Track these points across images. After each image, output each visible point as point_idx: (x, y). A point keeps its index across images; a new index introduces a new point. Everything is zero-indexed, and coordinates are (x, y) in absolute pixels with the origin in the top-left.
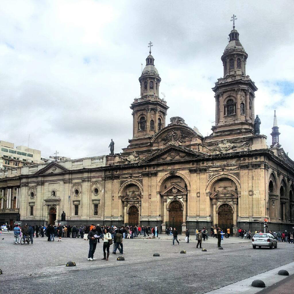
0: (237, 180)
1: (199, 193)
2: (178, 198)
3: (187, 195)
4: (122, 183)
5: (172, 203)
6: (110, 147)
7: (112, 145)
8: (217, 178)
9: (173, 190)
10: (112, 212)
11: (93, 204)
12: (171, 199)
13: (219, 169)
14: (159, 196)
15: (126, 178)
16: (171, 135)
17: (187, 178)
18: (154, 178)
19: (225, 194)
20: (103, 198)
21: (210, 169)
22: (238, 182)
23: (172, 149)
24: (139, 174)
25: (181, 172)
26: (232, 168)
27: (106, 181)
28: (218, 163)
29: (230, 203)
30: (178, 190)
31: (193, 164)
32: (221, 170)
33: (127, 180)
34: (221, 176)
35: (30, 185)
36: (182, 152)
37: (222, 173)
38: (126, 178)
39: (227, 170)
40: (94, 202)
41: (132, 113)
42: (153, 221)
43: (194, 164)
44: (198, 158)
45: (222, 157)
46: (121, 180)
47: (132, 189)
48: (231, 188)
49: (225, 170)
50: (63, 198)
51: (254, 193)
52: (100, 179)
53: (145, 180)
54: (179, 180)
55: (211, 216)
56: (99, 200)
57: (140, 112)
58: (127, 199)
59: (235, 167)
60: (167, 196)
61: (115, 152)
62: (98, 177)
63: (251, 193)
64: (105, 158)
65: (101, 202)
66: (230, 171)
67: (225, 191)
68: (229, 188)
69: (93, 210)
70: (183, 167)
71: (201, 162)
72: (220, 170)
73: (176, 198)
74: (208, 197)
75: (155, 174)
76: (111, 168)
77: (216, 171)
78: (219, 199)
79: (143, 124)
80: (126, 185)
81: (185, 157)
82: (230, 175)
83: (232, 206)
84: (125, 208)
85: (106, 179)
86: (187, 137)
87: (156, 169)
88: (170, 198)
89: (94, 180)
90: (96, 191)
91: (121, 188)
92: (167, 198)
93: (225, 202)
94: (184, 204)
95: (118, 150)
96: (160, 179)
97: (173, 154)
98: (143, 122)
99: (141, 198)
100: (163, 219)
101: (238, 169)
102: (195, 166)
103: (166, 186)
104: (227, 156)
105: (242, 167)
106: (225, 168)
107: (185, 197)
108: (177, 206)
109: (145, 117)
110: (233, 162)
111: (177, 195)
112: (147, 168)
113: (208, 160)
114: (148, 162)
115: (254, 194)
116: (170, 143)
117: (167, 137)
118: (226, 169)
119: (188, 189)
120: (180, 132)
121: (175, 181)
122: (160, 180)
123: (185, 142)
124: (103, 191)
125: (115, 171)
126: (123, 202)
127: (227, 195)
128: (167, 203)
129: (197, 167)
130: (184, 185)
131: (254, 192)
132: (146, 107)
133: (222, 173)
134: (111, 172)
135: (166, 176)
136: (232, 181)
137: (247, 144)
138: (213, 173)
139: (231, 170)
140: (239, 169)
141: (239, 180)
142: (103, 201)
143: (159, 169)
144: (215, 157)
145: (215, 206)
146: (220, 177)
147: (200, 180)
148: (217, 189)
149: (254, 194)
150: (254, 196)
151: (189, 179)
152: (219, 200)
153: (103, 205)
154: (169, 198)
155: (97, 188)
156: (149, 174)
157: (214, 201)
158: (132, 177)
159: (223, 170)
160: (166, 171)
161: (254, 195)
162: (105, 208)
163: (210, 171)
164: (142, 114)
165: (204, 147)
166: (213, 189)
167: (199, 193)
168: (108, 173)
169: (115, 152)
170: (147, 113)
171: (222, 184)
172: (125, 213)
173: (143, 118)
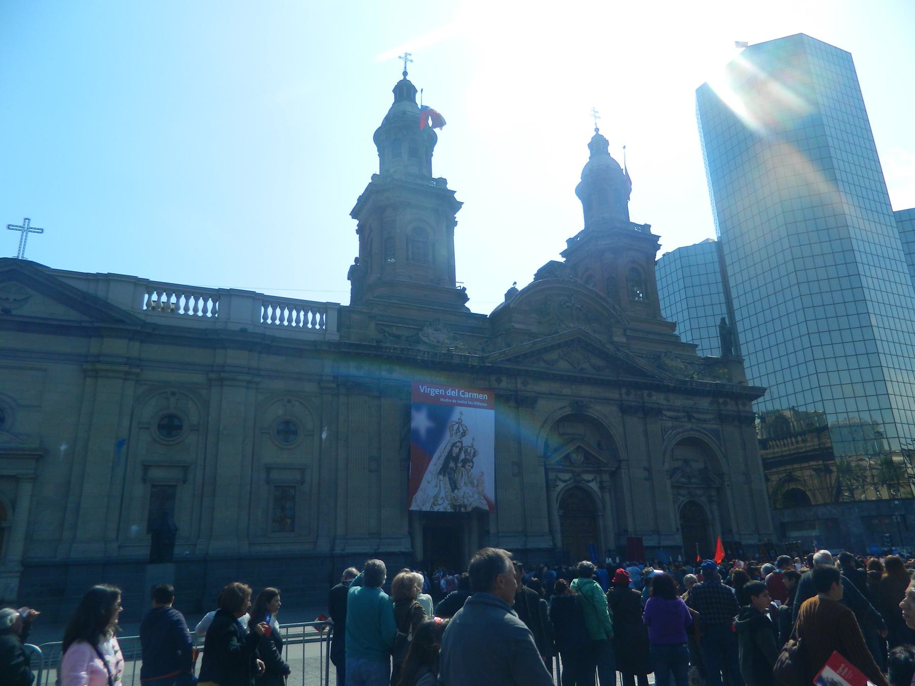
2: (584, 480)
11: (268, 482)
12: (565, 481)
28: (680, 401)
31: (628, 394)
32: (686, 419)
37: (689, 426)
49: (693, 420)
50: (63, 447)
56: (302, 470)
64: (334, 315)
71: (646, 392)
77: (676, 419)
88: (563, 478)
105: (722, 418)
107: (606, 477)
110: (705, 403)
112: (504, 379)
124: (324, 436)
133: (689, 426)
139: (705, 421)
163: (664, 418)
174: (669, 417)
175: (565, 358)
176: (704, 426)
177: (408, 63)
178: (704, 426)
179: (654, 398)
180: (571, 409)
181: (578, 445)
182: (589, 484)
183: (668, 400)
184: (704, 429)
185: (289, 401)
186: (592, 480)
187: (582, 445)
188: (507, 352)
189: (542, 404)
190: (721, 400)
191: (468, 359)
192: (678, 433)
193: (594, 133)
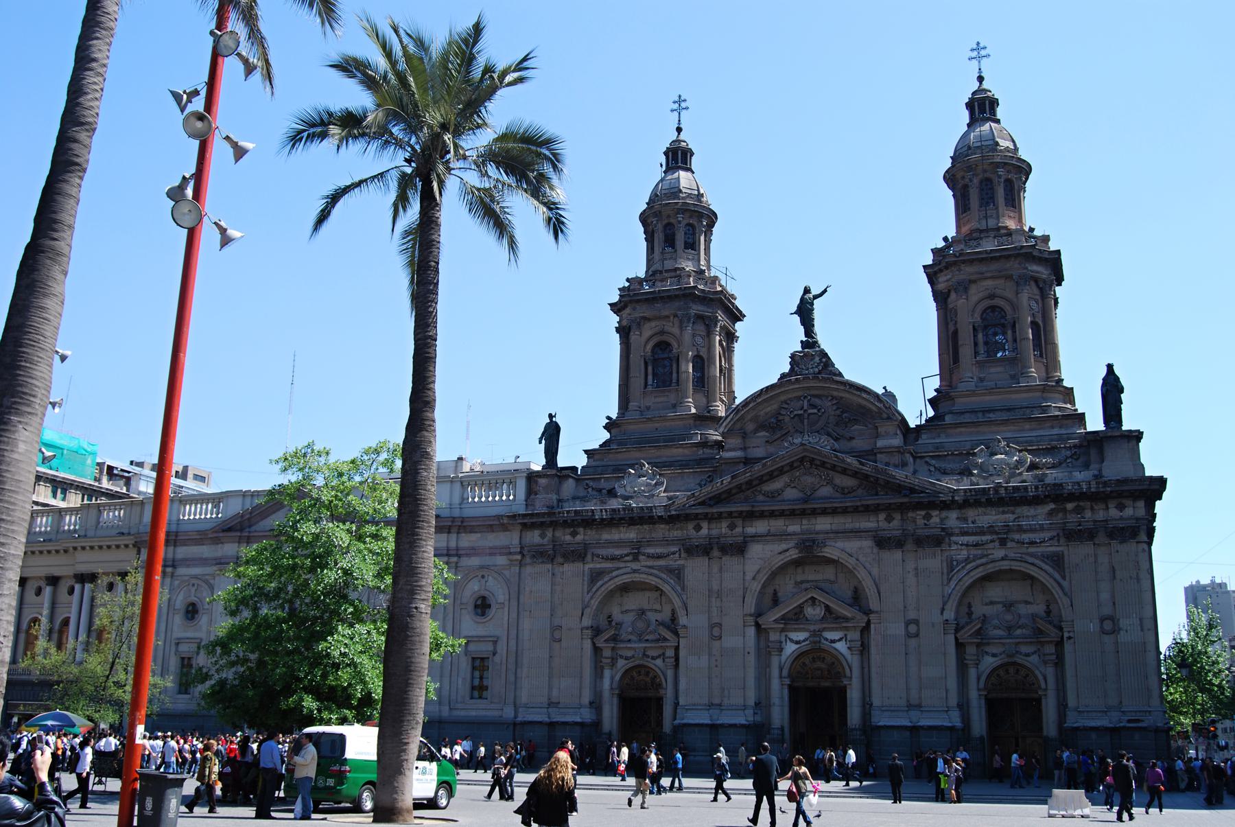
0: (1055, 580)
1: (916, 622)
2: (826, 639)
3: (866, 629)
4: (595, 576)
5: (799, 656)
6: (543, 441)
7: (551, 434)
8: (981, 569)
9: (809, 611)
10: (550, 688)
12: (797, 642)
13: (989, 537)
14: (751, 632)
15: (613, 558)
16: (801, 412)
17: (867, 565)
18: (731, 563)
19: (1009, 628)
20: (513, 632)
21: (954, 538)
22: (1059, 584)
23: (808, 461)
24: (668, 545)
25: (840, 544)
26: (1036, 537)
27: (528, 570)
29: (1031, 659)
30: (827, 608)
31: (889, 519)
32: (997, 544)
33: (618, 569)
34: (997, 564)
35: (181, 571)
36: (844, 471)
37: (1000, 553)
38: (613, 558)
39: (1018, 542)
40: (472, 647)
41: (617, 325)
42: (731, 726)
43: (894, 519)
44: (915, 498)
45: (1001, 499)
46: (591, 566)
47: (635, 601)
48: (1028, 606)
49: (1009, 544)
51: (1121, 626)
52: (501, 560)
53: (696, 570)
54: (829, 573)
55: (963, 706)
57: (653, 324)
58: (614, 639)
59: (1047, 535)
60: (783, 630)
61: (562, 461)
62: (494, 551)
63: (1108, 625)
64: (522, 485)
65: (502, 648)
66: (1027, 548)
67: (1009, 617)
68: (1023, 605)
69: (464, 679)
70: (849, 526)
72: (992, 541)
73: (820, 642)
74: (951, 638)
75: (739, 549)
76: (554, 519)
77: (976, 545)
78: (988, 644)
79: (665, 366)
80: (611, 585)
81: (854, 490)
82: (1031, 560)
83: (1037, 672)
84: (607, 673)
85: (528, 560)
86: (856, 421)
87: (739, 530)
88: (795, 638)
89: (475, 561)
90: (482, 606)
91: (592, 598)
92: (783, 639)
93: (1009, 656)
94: (854, 660)
95: (571, 455)
96: (756, 568)
97: (809, 480)
98: (663, 359)
99: (676, 634)
100: (769, 716)
101: (1058, 540)
102: (896, 523)
103: (775, 593)
104: (1020, 494)
105: (1072, 535)
106: (1012, 536)
107: (855, 635)
108: (818, 669)
109: (675, 344)
110: (1038, 515)
111: (824, 629)
112: (705, 525)
113: (946, 506)
114: (710, 506)
115: (1120, 629)
116: (798, 441)
117: (781, 418)
118: (1013, 540)
119: (874, 604)
120: (830, 404)
121: (811, 574)
122: (758, 572)
123: (852, 438)
125: (568, 531)
126: (597, 650)
127: (1019, 632)
128: (784, 658)
129: (904, 530)
130: (849, 593)
131: (1123, 623)
132: (680, 309)
133: (1000, 553)
134: (549, 534)
135: (782, 557)
136: (1032, 578)
137: (1077, 459)
138: (964, 553)
139: (1032, 543)
140: (1062, 540)
141: (1064, 578)
142: (513, 643)
143: (750, 530)
144: (974, 497)
145: (972, 672)
146: (991, 568)
147: (917, 575)
148: (979, 610)
149: (1120, 629)
150: (1123, 637)
151: (875, 571)
152: (987, 649)
153: (512, 659)
154: (792, 641)
155: (486, 594)
156: (712, 549)
157: (971, 650)
158: (641, 557)
159: (1003, 542)
160: (782, 536)
161: (1122, 632)
162: (519, 670)
164: (662, 332)
165: (918, 460)
166: (964, 609)
167: (916, 622)
168: (534, 537)
169: (562, 461)
170: (681, 328)
171: (996, 592)
172: (606, 694)
173: (663, 346)
174: (962, 545)
175: (793, 485)
176: (1032, 550)
177: (683, 113)
178: (1032, 550)
179: (935, 520)
180: (797, 551)
181: (809, 596)
182: (833, 645)
183: (965, 520)
184: (1032, 555)
185: (483, 577)
186: (840, 640)
187: (815, 596)
188: (696, 494)
189: (755, 550)
190: (1070, 506)
191: (652, 510)
192: (977, 567)
193: (976, 86)
